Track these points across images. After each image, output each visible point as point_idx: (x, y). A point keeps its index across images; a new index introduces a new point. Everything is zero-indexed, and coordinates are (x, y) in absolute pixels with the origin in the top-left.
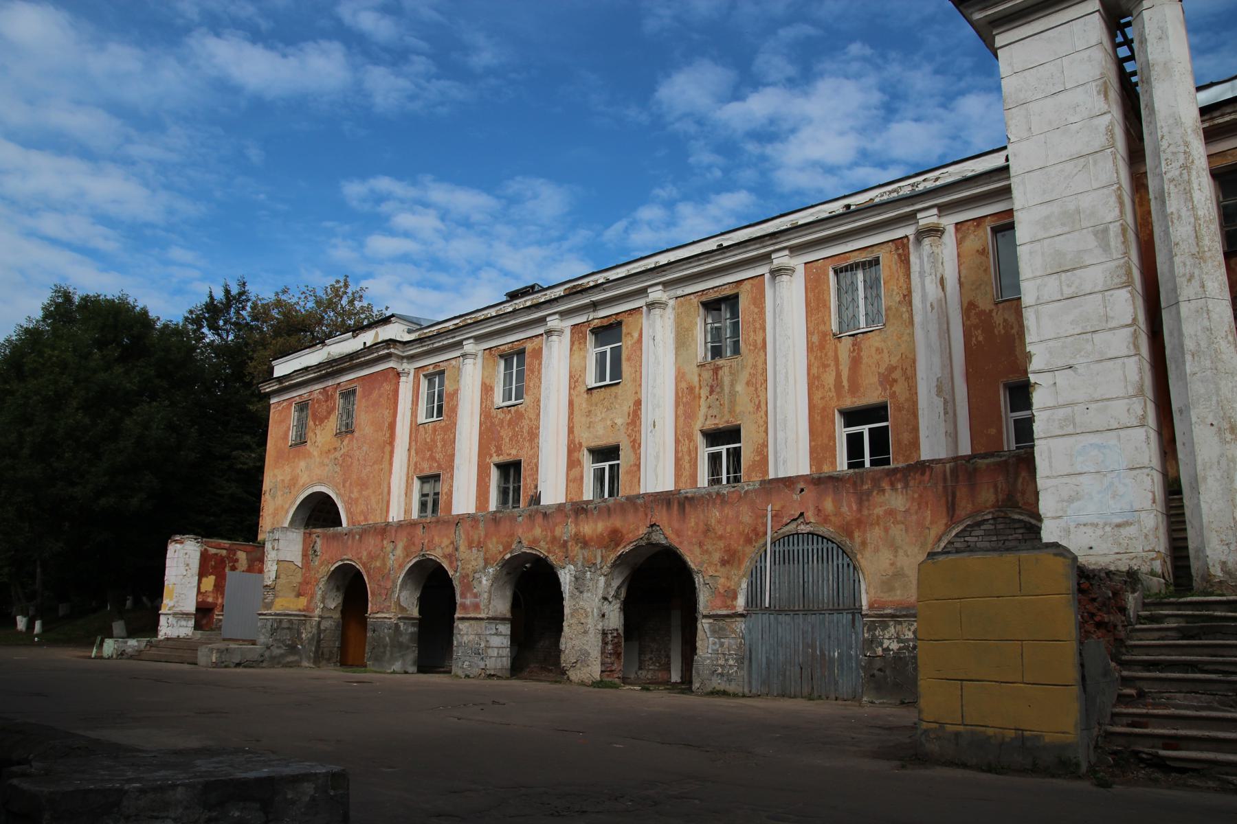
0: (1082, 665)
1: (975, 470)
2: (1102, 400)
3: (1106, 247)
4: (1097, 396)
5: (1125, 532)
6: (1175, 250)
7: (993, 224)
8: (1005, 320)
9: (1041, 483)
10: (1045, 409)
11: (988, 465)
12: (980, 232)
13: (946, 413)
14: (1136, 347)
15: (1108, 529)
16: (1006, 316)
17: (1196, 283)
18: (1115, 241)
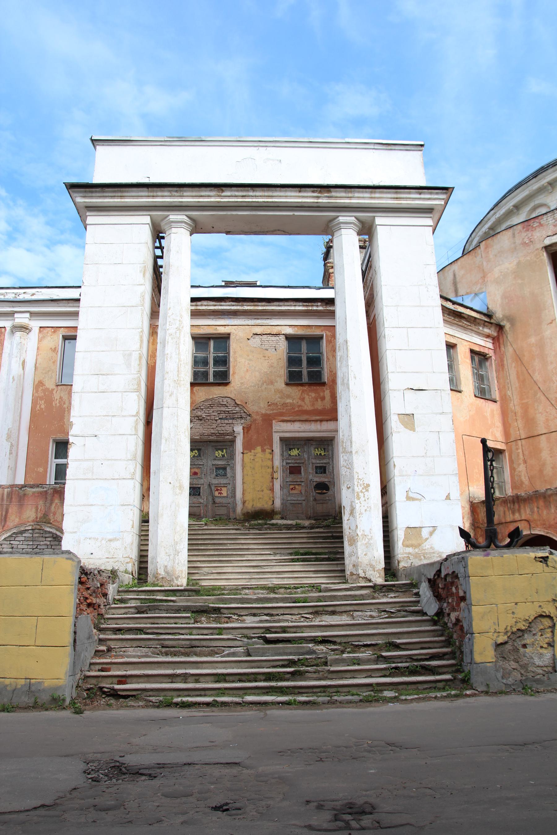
0: (75, 633)
1: (25, 495)
2: (111, 460)
6: (166, 376)
7: (64, 334)
8: (61, 398)
10: (76, 460)
11: (34, 493)
12: (55, 337)
13: (11, 453)
14: (136, 429)
15: (104, 542)
16: (62, 395)
18: (134, 363)
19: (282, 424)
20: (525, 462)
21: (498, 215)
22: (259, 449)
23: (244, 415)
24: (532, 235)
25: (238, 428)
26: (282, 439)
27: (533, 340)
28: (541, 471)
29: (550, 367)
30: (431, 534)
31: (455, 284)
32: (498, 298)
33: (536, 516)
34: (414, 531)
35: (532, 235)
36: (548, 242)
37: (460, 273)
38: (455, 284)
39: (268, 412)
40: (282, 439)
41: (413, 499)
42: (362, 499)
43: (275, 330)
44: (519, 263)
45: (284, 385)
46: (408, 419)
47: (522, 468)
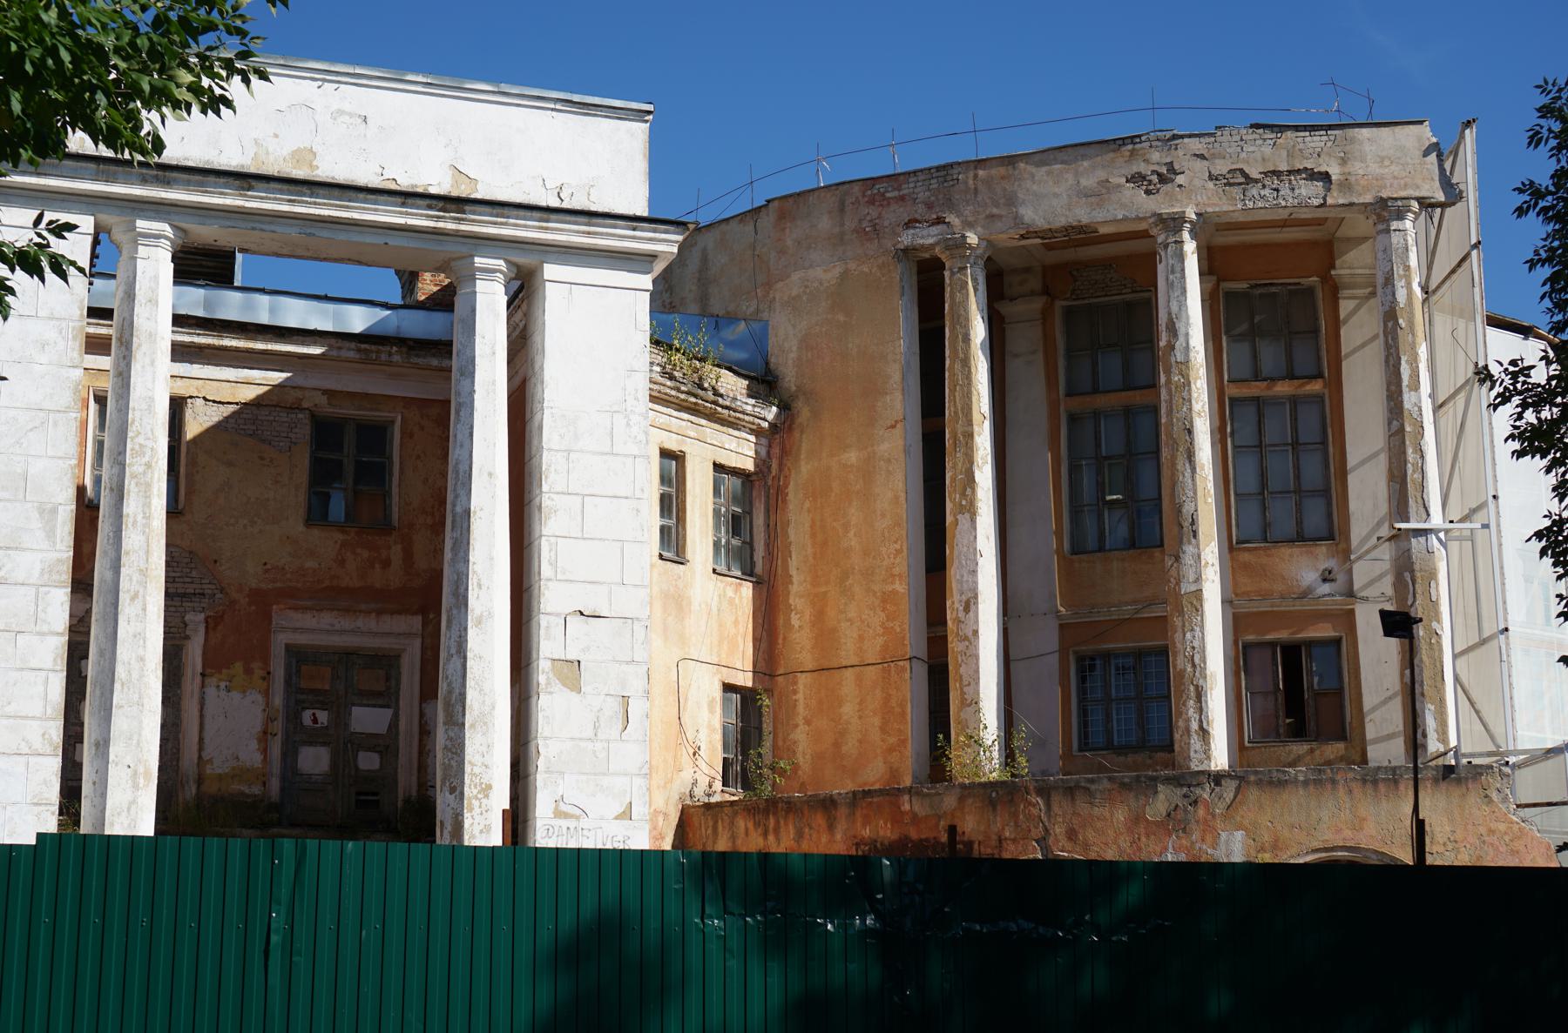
2: (15, 717)
3: (50, 534)
17: (138, 603)
19: (292, 614)
20: (808, 722)
22: (238, 667)
24: (879, 217)
27: (852, 457)
28: (837, 745)
35: (879, 217)
36: (906, 238)
39: (263, 586)
41: (566, 816)
42: (477, 810)
44: (844, 276)
45: (301, 528)
46: (571, 670)
47: (801, 736)
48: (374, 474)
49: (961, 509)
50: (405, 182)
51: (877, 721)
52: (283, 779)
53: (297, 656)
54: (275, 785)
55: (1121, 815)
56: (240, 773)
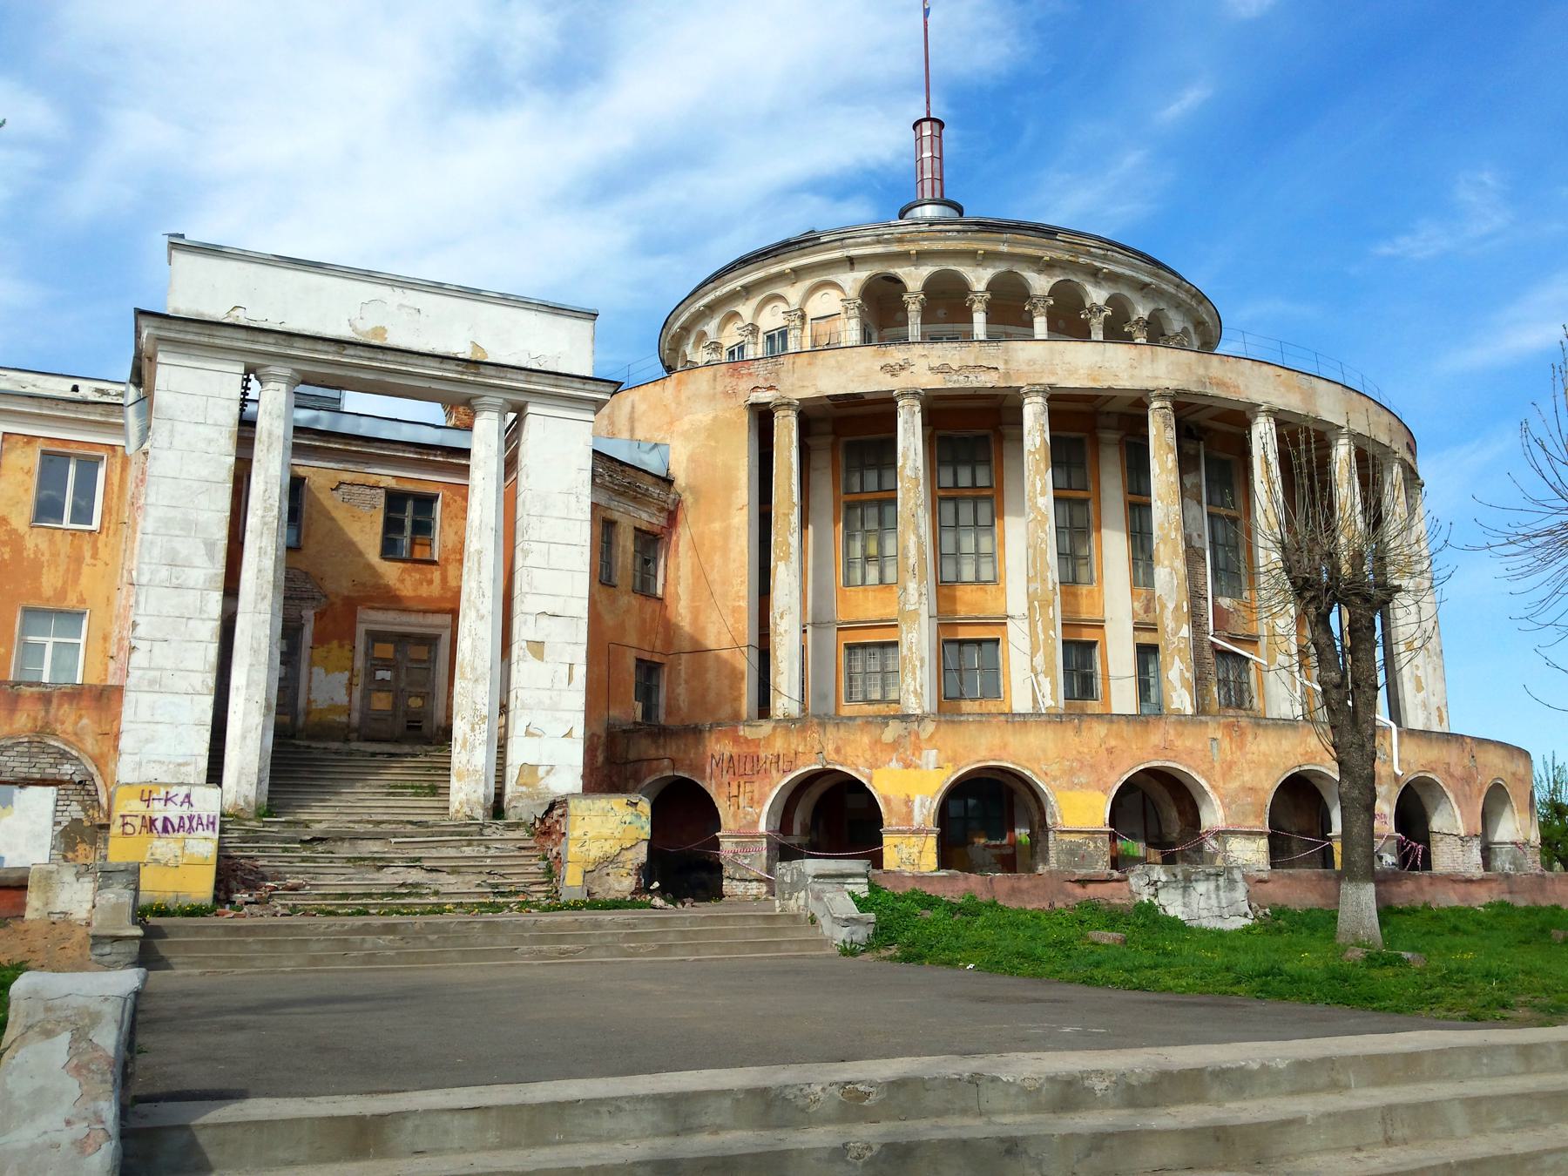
1: (18, 695)
3: (211, 557)
4: (181, 666)
5: (183, 769)
9: (124, 726)
12: (29, 450)
16: (39, 541)
20: (686, 682)
21: (718, 293)
22: (335, 644)
23: (317, 595)
25: (309, 614)
26: (369, 633)
27: (717, 526)
29: (733, 566)
30: (548, 773)
31: (632, 419)
32: (684, 458)
33: (681, 755)
34: (529, 770)
37: (642, 407)
38: (632, 419)
40: (369, 633)
41: (533, 735)
43: (372, 480)
44: (715, 419)
46: (537, 648)
47: (682, 690)
48: (423, 528)
49: (781, 559)
50: (440, 350)
51: (727, 682)
52: (362, 712)
53: (375, 637)
54: (356, 717)
55: (866, 740)
56: (334, 709)
